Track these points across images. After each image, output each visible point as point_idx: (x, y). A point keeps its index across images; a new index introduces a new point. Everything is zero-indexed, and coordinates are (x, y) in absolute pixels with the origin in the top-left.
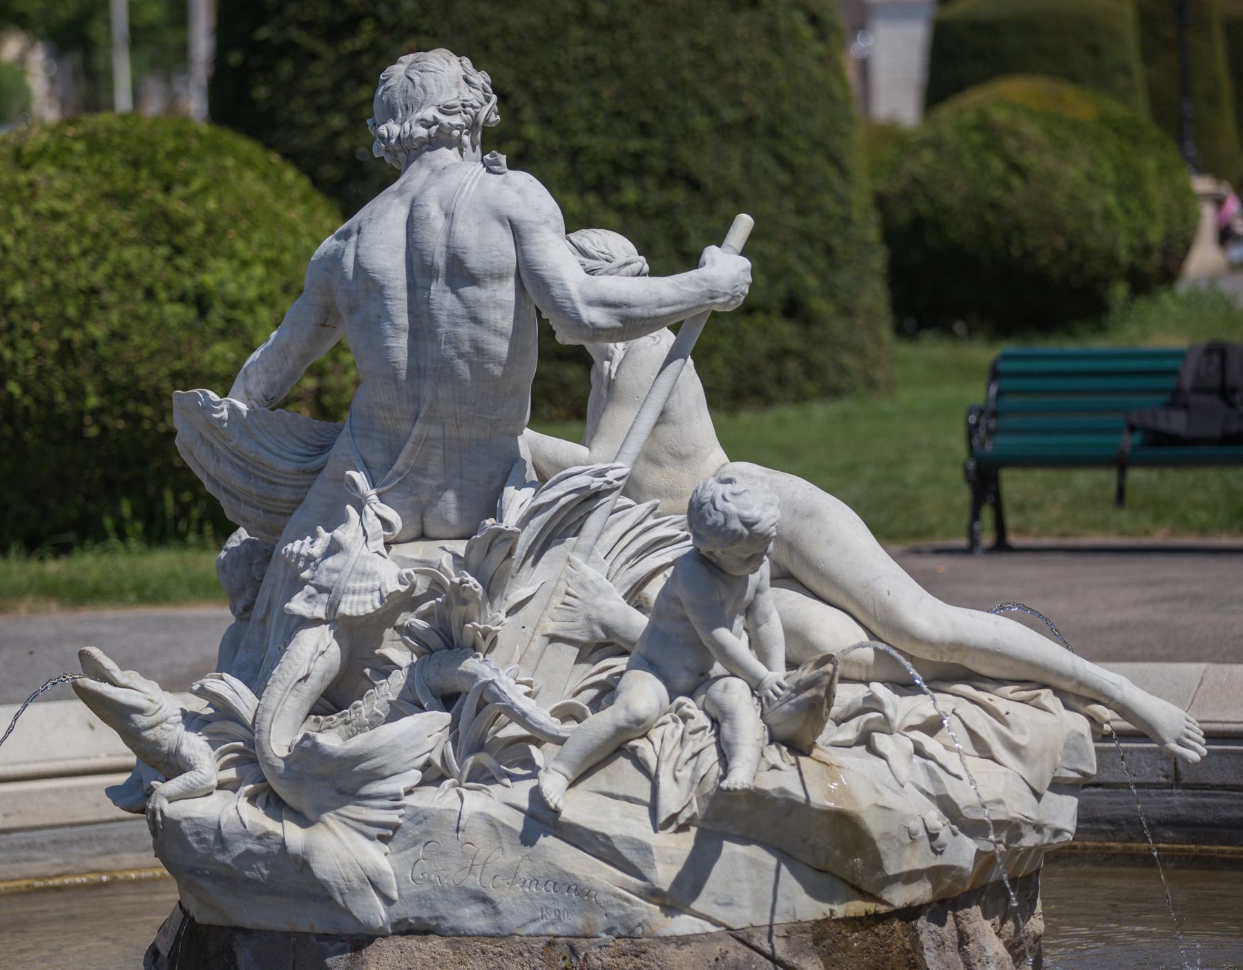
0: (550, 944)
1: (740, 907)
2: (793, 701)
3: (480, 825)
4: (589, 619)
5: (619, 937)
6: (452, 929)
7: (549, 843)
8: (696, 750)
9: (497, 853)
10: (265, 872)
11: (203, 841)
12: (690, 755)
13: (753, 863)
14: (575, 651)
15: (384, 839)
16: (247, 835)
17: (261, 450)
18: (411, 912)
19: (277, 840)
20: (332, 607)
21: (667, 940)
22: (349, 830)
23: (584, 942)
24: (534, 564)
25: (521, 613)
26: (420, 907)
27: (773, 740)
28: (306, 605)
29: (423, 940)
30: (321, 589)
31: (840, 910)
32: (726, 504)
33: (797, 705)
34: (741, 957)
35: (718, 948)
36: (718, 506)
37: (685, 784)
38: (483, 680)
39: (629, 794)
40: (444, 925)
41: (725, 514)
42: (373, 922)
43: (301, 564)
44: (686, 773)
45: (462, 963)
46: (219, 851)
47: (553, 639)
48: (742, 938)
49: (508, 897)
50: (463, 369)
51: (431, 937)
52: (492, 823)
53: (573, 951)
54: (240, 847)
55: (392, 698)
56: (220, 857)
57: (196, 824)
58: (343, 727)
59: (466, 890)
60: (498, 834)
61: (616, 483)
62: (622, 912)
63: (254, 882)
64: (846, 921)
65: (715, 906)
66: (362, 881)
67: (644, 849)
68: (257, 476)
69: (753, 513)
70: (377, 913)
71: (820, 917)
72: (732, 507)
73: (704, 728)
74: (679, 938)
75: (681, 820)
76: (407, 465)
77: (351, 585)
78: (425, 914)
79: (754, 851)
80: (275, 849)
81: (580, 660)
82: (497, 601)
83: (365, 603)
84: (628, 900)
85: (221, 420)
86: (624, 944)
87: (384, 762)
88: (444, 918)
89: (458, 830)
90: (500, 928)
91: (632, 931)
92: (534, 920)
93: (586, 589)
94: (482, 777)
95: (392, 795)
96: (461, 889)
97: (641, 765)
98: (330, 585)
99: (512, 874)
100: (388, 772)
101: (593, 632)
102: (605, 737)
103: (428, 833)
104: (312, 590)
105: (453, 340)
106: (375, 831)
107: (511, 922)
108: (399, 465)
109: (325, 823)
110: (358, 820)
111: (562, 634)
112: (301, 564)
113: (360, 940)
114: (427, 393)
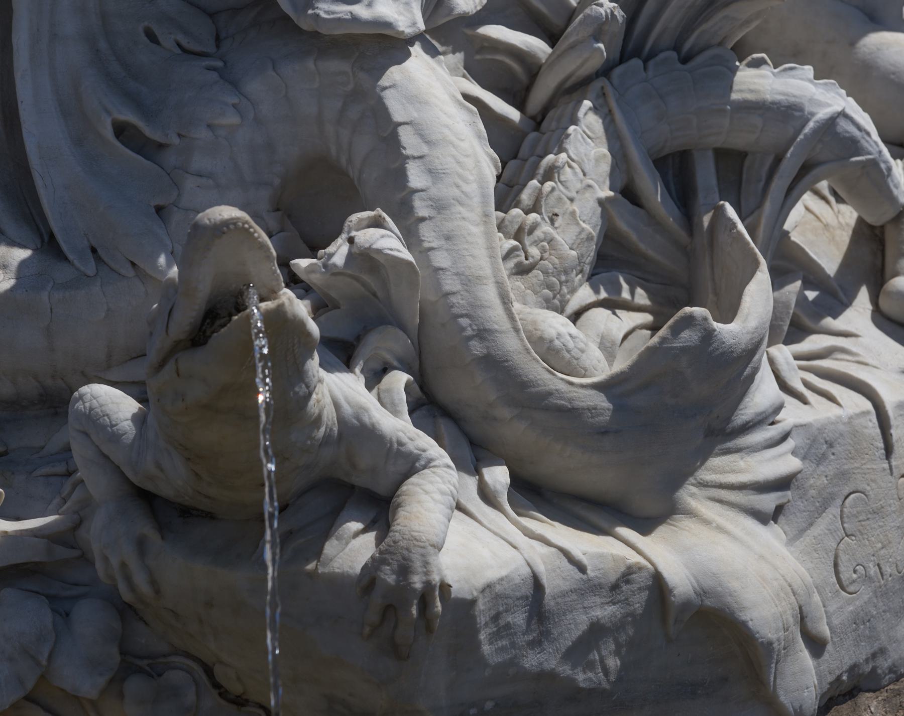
10: (613, 663)
11: (503, 631)
19: (641, 579)
38: (822, 114)
46: (532, 644)
54: (577, 623)
56: (531, 661)
57: (498, 597)
63: (593, 692)
80: (639, 602)
89: (889, 450)
103: (843, 475)
106: (768, 502)
109: (690, 513)
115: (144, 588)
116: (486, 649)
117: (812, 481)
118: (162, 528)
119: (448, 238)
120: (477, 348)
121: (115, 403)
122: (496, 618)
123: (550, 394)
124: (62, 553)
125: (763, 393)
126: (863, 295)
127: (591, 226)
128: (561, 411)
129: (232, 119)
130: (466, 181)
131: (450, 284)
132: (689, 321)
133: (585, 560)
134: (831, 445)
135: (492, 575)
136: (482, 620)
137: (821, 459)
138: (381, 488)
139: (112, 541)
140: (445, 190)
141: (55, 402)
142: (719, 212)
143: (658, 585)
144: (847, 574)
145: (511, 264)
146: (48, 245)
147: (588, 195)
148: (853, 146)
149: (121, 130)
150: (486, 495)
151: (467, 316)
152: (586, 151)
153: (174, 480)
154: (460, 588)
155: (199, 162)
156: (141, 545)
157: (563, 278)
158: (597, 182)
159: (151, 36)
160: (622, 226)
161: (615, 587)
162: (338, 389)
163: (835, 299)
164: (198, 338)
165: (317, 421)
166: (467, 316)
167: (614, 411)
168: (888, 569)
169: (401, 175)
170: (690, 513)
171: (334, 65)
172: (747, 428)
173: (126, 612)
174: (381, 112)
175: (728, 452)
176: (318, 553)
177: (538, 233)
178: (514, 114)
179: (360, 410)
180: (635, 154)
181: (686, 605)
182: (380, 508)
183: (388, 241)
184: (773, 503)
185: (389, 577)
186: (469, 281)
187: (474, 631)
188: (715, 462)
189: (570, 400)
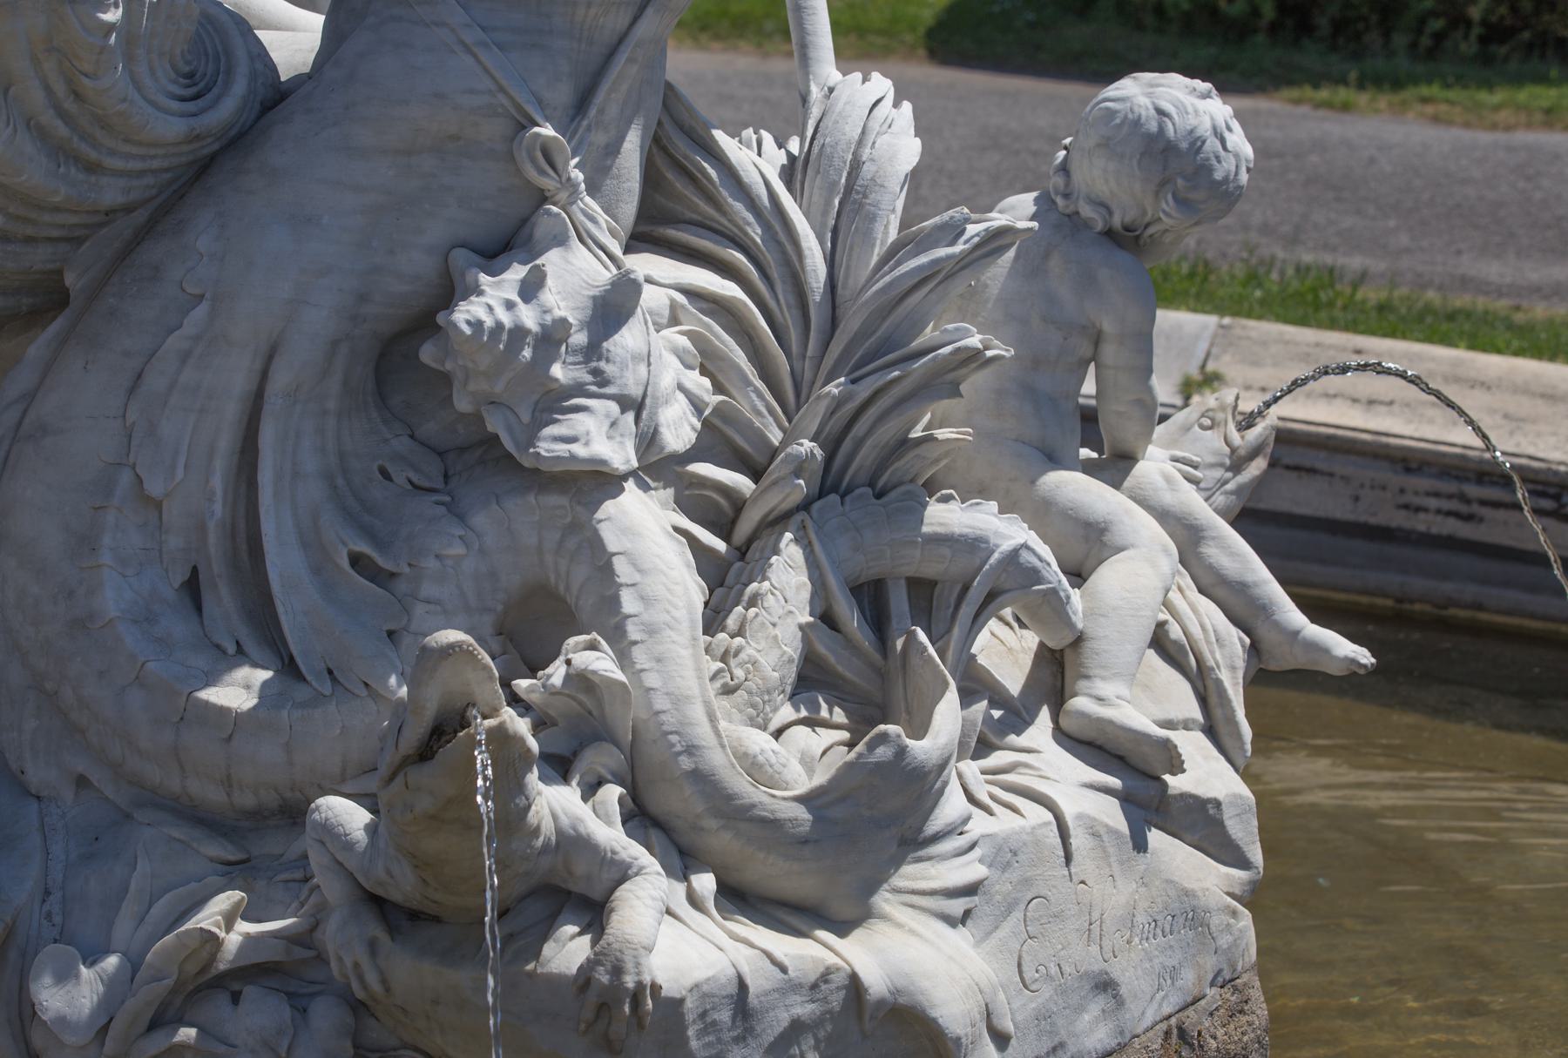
2: (1229, 487)
11: (710, 1027)
16: (794, 987)
19: (839, 979)
23: (1190, 1012)
38: (1006, 546)
43: (527, 353)
53: (1182, 1033)
54: (780, 1019)
57: (705, 996)
80: (836, 1001)
85: (111, 27)
89: (1068, 858)
98: (635, 391)
104: (614, 407)
106: (957, 906)
109: (884, 917)
110: (933, 893)
112: (527, 353)
115: (376, 987)
116: (694, 1044)
118: (392, 930)
119: (659, 660)
120: (686, 763)
121: (347, 814)
122: (703, 1015)
123: (753, 806)
124: (300, 953)
125: (952, 805)
126: (1044, 715)
127: (792, 648)
128: (764, 821)
129: (458, 550)
130: (676, 607)
131: (660, 703)
132: (883, 738)
133: (786, 962)
134: (1015, 854)
135: (700, 974)
136: (690, 1017)
137: (1006, 867)
138: (596, 894)
139: (347, 942)
140: (657, 616)
141: (293, 813)
142: (911, 636)
143: (854, 984)
144: (1029, 974)
145: (718, 684)
146: (288, 668)
147: (789, 620)
148: (1034, 576)
149: (356, 560)
150: (694, 901)
151: (676, 733)
152: (787, 580)
153: (403, 886)
154: (670, 989)
155: (428, 589)
156: (372, 947)
159: (384, 473)
160: (821, 649)
161: (814, 987)
162: (555, 803)
163: (1017, 717)
164: (425, 753)
165: (536, 831)
166: (676, 733)
167: (814, 822)
168: (1067, 969)
169: (615, 602)
170: (884, 917)
171: (553, 500)
172: (936, 838)
173: (358, 1008)
174: (596, 543)
175: (920, 860)
176: (537, 954)
177: (743, 656)
178: (720, 545)
179: (576, 821)
180: (833, 582)
181: (881, 1002)
182: (594, 912)
183: (602, 663)
184: (962, 906)
185: (602, 976)
186: (678, 700)
187: (683, 1028)
188: (908, 869)
189: (772, 812)
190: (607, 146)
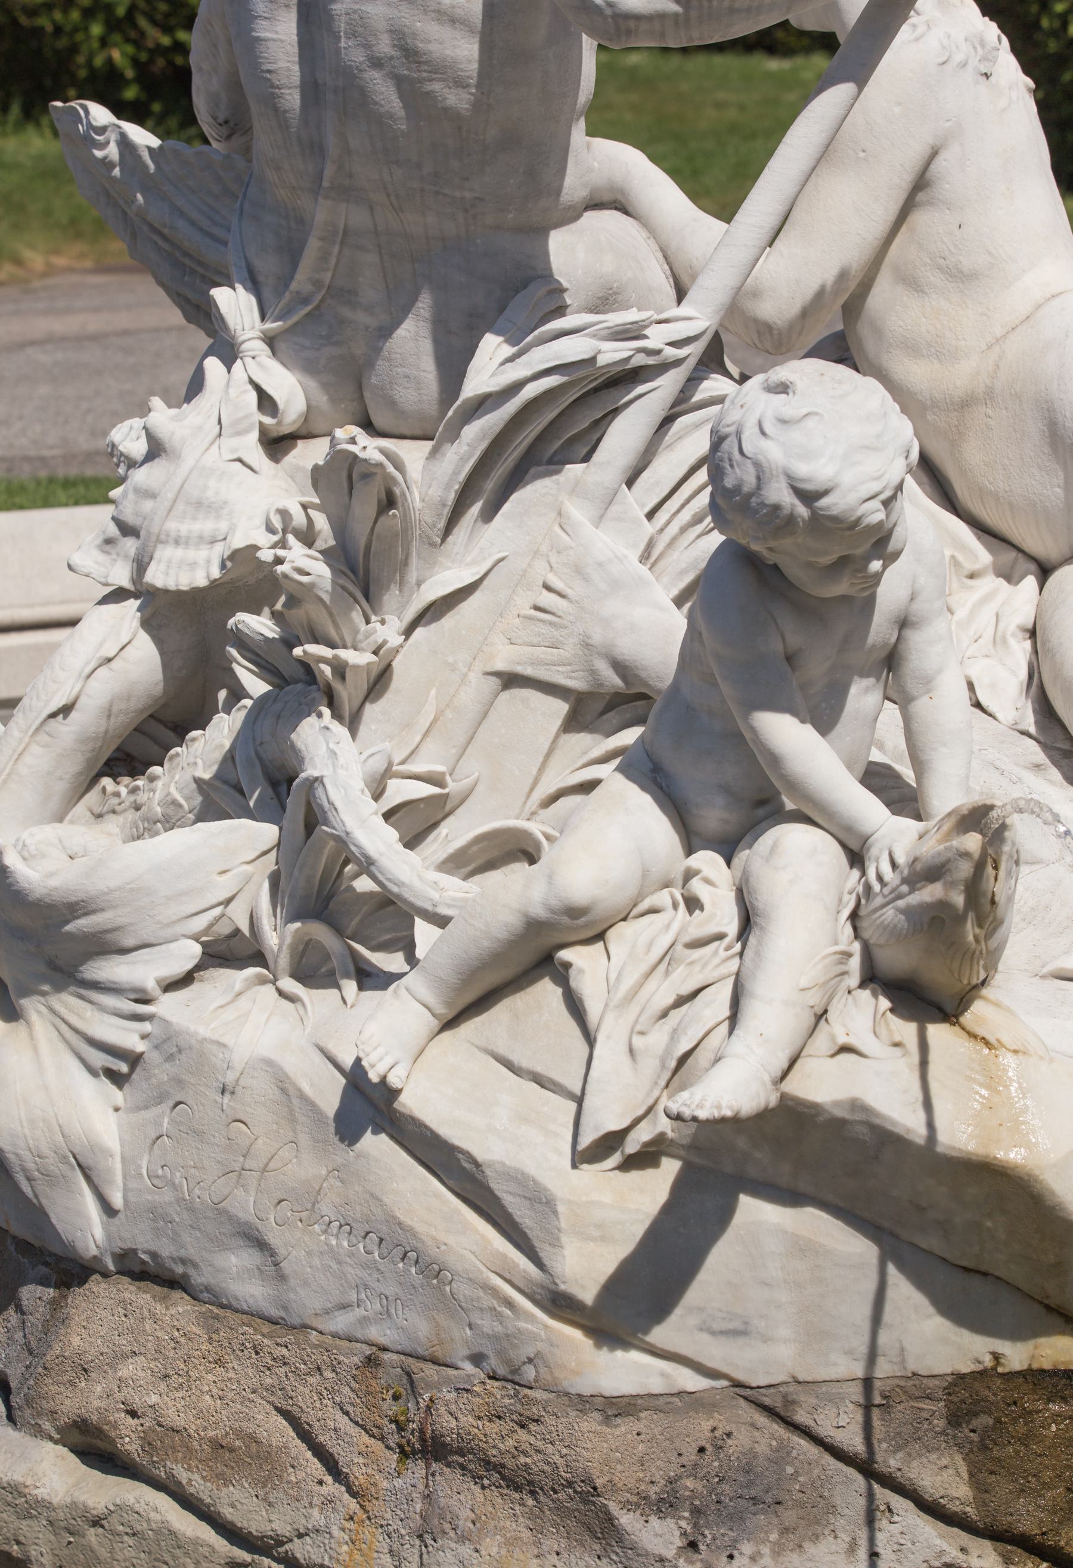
0: (371, 1362)
1: (766, 1339)
2: (901, 903)
3: (260, 1086)
4: (586, 645)
5: (493, 1377)
6: (208, 1289)
7: (376, 1145)
8: (686, 989)
9: (286, 1153)
12: (670, 1000)
13: (802, 1247)
14: (561, 708)
15: (117, 1079)
17: (181, 224)
18: (143, 1240)
20: (141, 565)
21: (584, 1403)
22: (61, 1046)
23: (430, 1371)
24: (489, 513)
25: (448, 621)
26: (157, 1232)
27: (871, 978)
28: (101, 557)
29: (163, 1299)
30: (127, 530)
31: (1017, 1355)
32: (765, 444)
33: (907, 912)
34: (762, 1449)
35: (706, 1425)
36: (747, 448)
37: (649, 1066)
39: (539, 1069)
40: (198, 1279)
41: (757, 465)
42: (80, 1246)
44: (657, 1038)
45: (219, 1362)
47: (511, 680)
48: (777, 1407)
49: (299, 1246)
50: (385, 94)
51: (177, 1295)
52: (285, 1087)
55: (207, 774)
58: (131, 815)
59: (231, 1218)
60: (291, 1112)
61: (671, 353)
62: (498, 1328)
64: (1034, 1377)
65: (705, 1337)
66: (64, 1159)
67: (543, 1201)
68: (193, 272)
69: (815, 471)
70: (88, 1230)
71: (966, 1368)
72: (773, 452)
73: (720, 937)
74: (610, 1401)
75: (632, 1145)
76: (317, 284)
77: (172, 525)
78: (166, 1250)
79: (813, 1223)
81: (573, 723)
82: (391, 598)
83: (193, 565)
84: (509, 1304)
86: (501, 1395)
87: (121, 921)
88: (195, 1266)
90: (285, 1308)
91: (516, 1371)
92: (344, 1307)
93: (587, 580)
94: (312, 970)
95: (135, 990)
96: (223, 1214)
97: (575, 1006)
99: (306, 1203)
100: (129, 941)
101: (593, 672)
102: (502, 934)
103: (179, 1082)
105: (360, 30)
106: (100, 1059)
107: (307, 1301)
108: (301, 281)
110: (76, 1031)
111: (529, 671)
113: (70, 1271)
114: (331, 141)
117: (157, 1071)
134: (180, 1051)
137: (170, 1058)
157: (146, 825)
158: (204, 763)
175: (82, 997)
190: (380, 329)
